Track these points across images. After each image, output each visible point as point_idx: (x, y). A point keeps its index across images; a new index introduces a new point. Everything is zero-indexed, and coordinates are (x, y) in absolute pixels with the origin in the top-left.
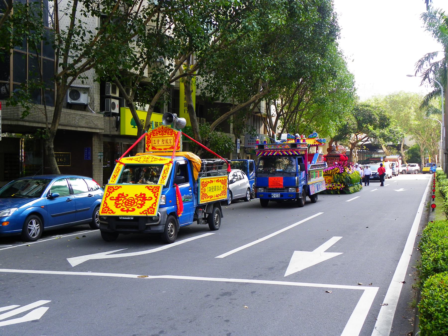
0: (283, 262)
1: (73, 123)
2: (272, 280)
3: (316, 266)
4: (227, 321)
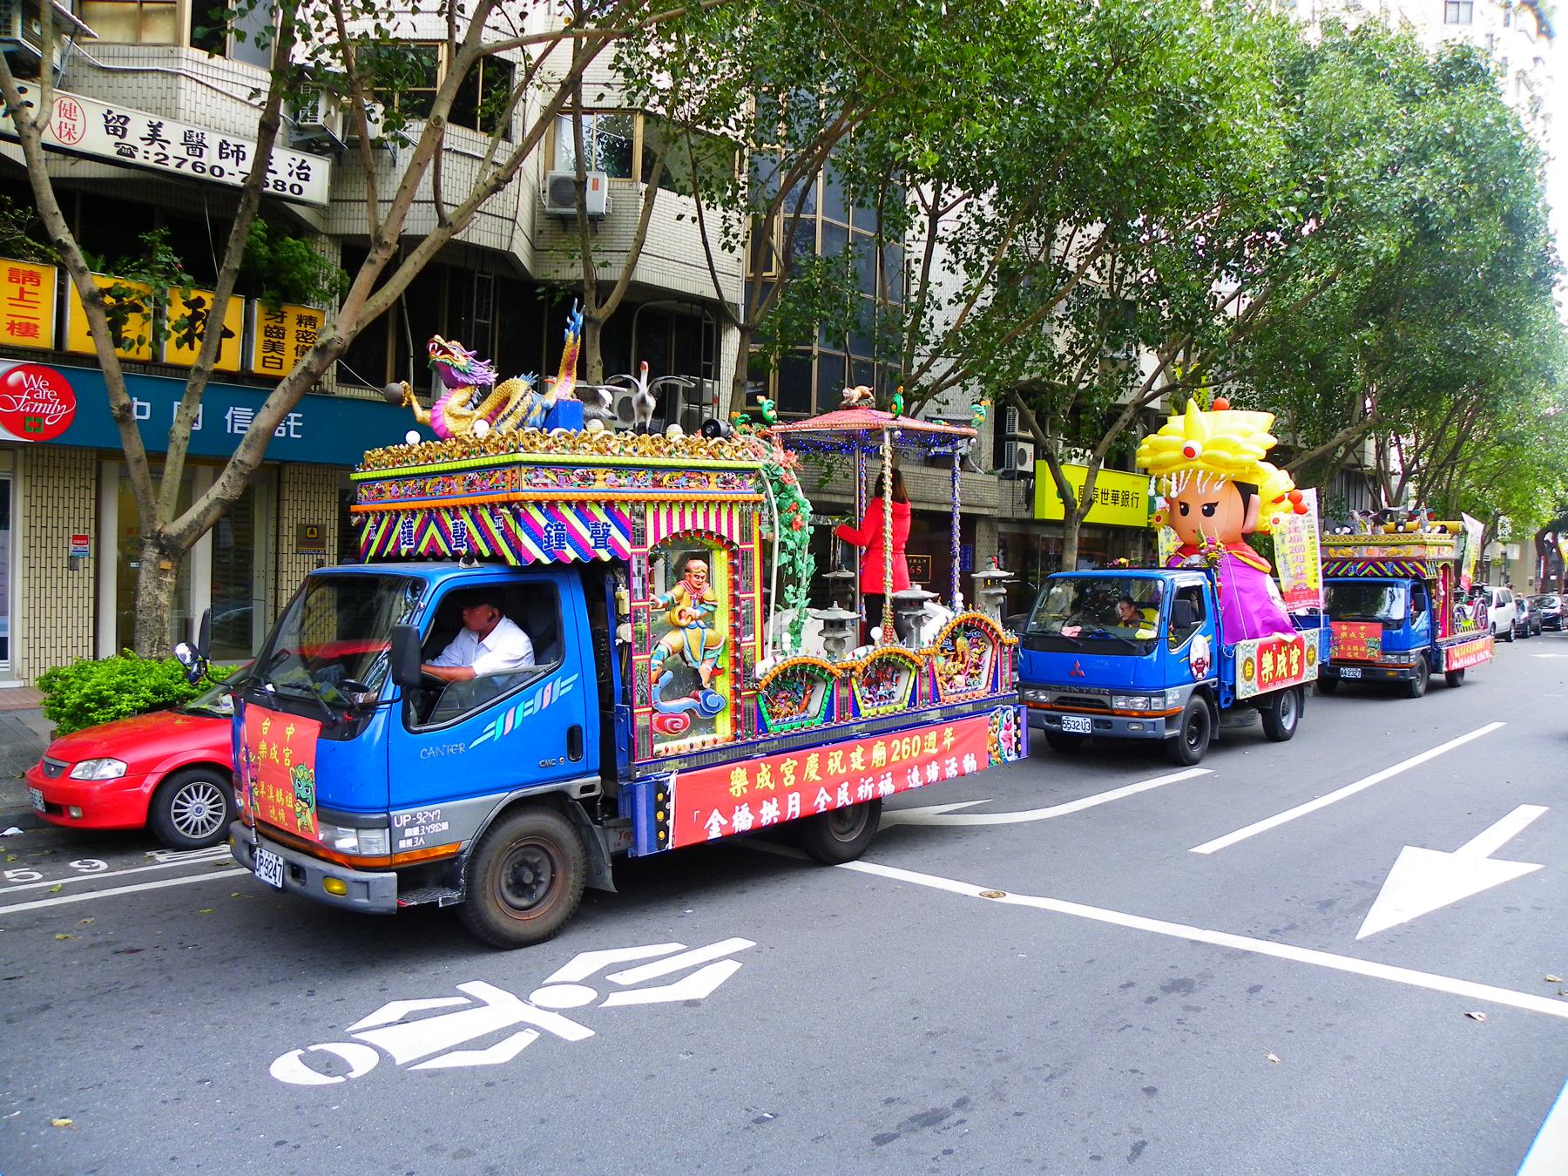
0: (1364, 884)
1: (931, 496)
2: (1322, 948)
3: (1455, 907)
4: (1150, 1091)
